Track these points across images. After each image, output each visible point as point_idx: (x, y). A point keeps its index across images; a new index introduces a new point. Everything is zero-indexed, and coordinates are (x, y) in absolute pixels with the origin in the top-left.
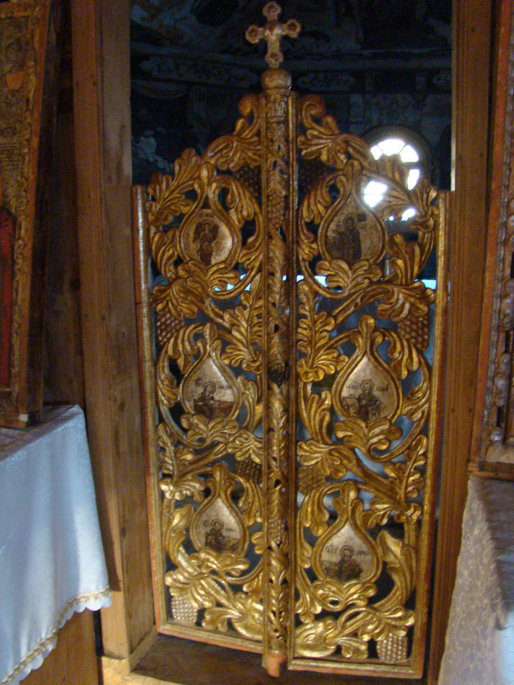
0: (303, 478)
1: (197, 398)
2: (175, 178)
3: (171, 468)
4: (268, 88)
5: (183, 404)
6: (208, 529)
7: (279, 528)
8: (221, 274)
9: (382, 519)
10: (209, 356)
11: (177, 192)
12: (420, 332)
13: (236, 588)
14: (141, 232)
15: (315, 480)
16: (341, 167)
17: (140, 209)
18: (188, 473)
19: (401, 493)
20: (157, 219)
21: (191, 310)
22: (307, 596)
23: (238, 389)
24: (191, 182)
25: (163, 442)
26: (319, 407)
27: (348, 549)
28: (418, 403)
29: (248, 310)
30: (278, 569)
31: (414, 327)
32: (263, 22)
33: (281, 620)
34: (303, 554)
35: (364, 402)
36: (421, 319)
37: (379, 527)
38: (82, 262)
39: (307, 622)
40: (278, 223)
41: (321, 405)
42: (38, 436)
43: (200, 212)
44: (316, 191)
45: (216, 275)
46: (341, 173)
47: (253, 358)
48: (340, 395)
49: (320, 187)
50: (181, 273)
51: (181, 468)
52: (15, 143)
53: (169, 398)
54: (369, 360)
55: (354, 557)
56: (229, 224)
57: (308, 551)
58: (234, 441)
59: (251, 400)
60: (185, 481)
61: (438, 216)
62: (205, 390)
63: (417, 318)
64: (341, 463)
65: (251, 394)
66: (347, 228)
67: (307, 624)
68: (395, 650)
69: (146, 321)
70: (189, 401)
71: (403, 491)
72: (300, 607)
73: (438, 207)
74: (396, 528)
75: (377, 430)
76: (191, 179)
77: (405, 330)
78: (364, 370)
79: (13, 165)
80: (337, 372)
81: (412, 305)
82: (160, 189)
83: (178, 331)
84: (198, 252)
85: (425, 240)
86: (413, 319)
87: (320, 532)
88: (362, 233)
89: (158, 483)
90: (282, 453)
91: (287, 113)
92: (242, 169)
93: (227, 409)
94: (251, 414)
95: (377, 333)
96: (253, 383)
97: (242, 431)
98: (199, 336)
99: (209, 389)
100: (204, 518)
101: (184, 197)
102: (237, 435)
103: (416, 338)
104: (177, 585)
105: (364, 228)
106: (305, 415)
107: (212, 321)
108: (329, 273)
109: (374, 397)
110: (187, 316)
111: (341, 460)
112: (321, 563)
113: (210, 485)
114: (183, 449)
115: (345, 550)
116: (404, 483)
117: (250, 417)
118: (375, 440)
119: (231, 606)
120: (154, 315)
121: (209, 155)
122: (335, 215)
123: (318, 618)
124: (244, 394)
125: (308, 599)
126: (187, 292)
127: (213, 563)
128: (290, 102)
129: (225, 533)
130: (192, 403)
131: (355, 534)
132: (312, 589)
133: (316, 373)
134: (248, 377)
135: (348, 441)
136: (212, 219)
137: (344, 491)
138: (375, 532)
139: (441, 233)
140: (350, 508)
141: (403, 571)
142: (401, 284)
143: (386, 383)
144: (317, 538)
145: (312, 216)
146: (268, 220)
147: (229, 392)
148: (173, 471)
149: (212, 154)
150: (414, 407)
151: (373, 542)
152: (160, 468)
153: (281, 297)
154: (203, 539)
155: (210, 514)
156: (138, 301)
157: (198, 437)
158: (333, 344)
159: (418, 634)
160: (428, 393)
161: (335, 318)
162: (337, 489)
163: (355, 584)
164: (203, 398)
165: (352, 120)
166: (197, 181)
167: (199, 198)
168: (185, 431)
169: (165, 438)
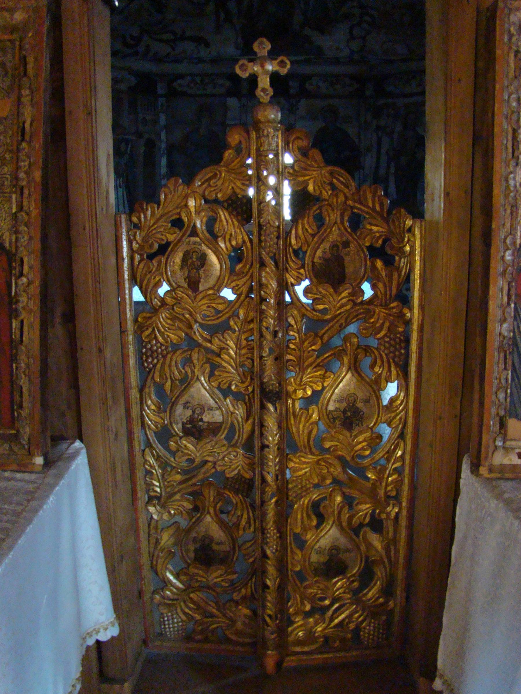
0: (293, 488)
1: (185, 421)
2: (161, 206)
3: (158, 490)
4: (261, 122)
5: (170, 428)
6: (198, 545)
7: (275, 537)
8: (210, 300)
9: (365, 518)
10: (198, 379)
11: (162, 220)
12: (398, 347)
14: (126, 261)
15: (304, 489)
16: (327, 197)
17: (124, 237)
18: (175, 493)
19: (382, 492)
20: (141, 247)
21: (178, 336)
22: (298, 596)
23: (227, 410)
24: (178, 211)
25: (151, 466)
26: (308, 421)
27: (334, 549)
28: (396, 410)
29: (237, 333)
30: (275, 576)
31: (392, 342)
32: (253, 57)
33: (278, 621)
34: (293, 558)
35: (349, 414)
36: (398, 336)
37: (361, 525)
38: (77, 295)
39: (297, 620)
40: (272, 252)
41: (310, 419)
42: (59, 477)
43: (187, 240)
44: (303, 220)
45: (204, 302)
46: (327, 203)
47: (241, 379)
48: (326, 408)
49: (306, 216)
51: (169, 489)
52: (6, 174)
53: (155, 422)
54: (353, 375)
55: (340, 555)
56: (217, 253)
57: (299, 555)
58: (223, 458)
59: (240, 419)
60: (174, 501)
61: (414, 243)
62: (194, 412)
63: (395, 335)
64: (328, 472)
65: (240, 412)
66: (332, 254)
67: (298, 621)
68: (376, 634)
69: (131, 348)
70: (177, 424)
71: (383, 491)
72: (291, 607)
73: (414, 235)
74: (376, 524)
75: (361, 438)
76: (177, 208)
77: (384, 346)
78: (349, 384)
79: (5, 197)
80: (324, 388)
81: (391, 323)
82: (145, 217)
83: (164, 357)
84: (185, 279)
85: (402, 264)
86: (392, 336)
87: (308, 536)
88: (347, 259)
89: (146, 506)
90: (277, 468)
91: (277, 146)
92: (230, 198)
93: (214, 429)
94: (239, 432)
95: (359, 351)
96: (243, 403)
97: (230, 449)
98: (188, 361)
99: (198, 411)
100: (194, 534)
101: (170, 224)
102: (225, 453)
103: (394, 353)
104: (166, 601)
105: (348, 254)
106: (294, 430)
107: (199, 345)
108: (316, 296)
109: (358, 408)
110: (175, 341)
111: (328, 468)
112: (310, 564)
113: (199, 503)
114: (171, 471)
115: (332, 549)
116: (384, 484)
117: (239, 436)
118: (360, 446)
119: (220, 615)
120: (140, 343)
121: (196, 184)
122: (321, 243)
124: (232, 413)
125: (299, 598)
126: (174, 318)
127: (202, 577)
128: (280, 136)
129: (215, 547)
130: (180, 425)
131: (341, 533)
132: (302, 589)
133: (304, 389)
134: (238, 397)
135: (333, 451)
136: (199, 247)
137: (330, 495)
138: (356, 530)
139: (417, 258)
140: (336, 512)
141: (383, 563)
142: (381, 305)
143: (368, 394)
144: (306, 542)
145: (300, 245)
147: (218, 412)
148: (161, 494)
149: (200, 183)
150: (393, 415)
151: (357, 540)
152: (147, 491)
153: (274, 322)
156: (123, 329)
157: (187, 457)
158: (319, 363)
159: (397, 617)
160: (405, 402)
161: (321, 337)
162: (324, 495)
163: (341, 580)
164: (191, 420)
165: (227, 122)
166: (183, 210)
167: (186, 226)
168: (173, 454)
169: (152, 461)
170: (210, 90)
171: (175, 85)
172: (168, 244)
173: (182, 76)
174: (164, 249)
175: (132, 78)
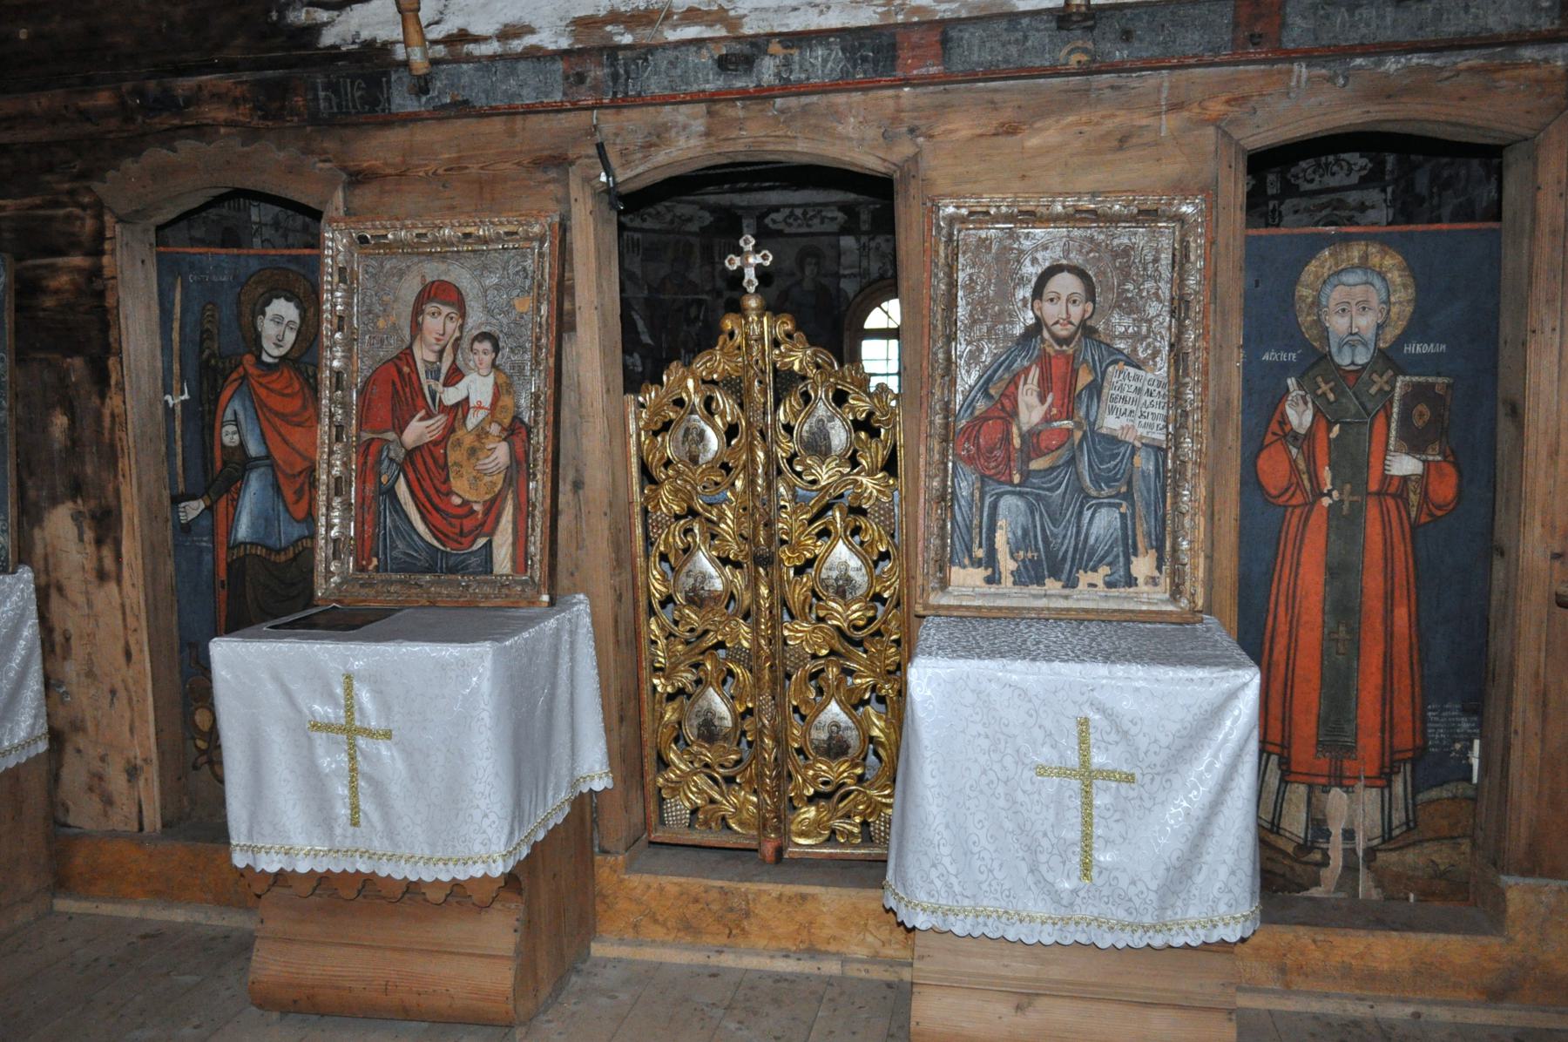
13: (730, 780)
50: (671, 472)
56: (714, 427)
65: (739, 580)
93: (715, 597)
98: (688, 531)
100: (697, 708)
123: (811, 800)
134: (737, 565)
146: (749, 423)
154: (695, 731)
155: (703, 703)
164: (694, 589)
165: (842, 272)
170: (816, 226)
171: (767, 221)
172: (671, 421)
173: (776, 209)
174: (666, 426)
175: (707, 214)
